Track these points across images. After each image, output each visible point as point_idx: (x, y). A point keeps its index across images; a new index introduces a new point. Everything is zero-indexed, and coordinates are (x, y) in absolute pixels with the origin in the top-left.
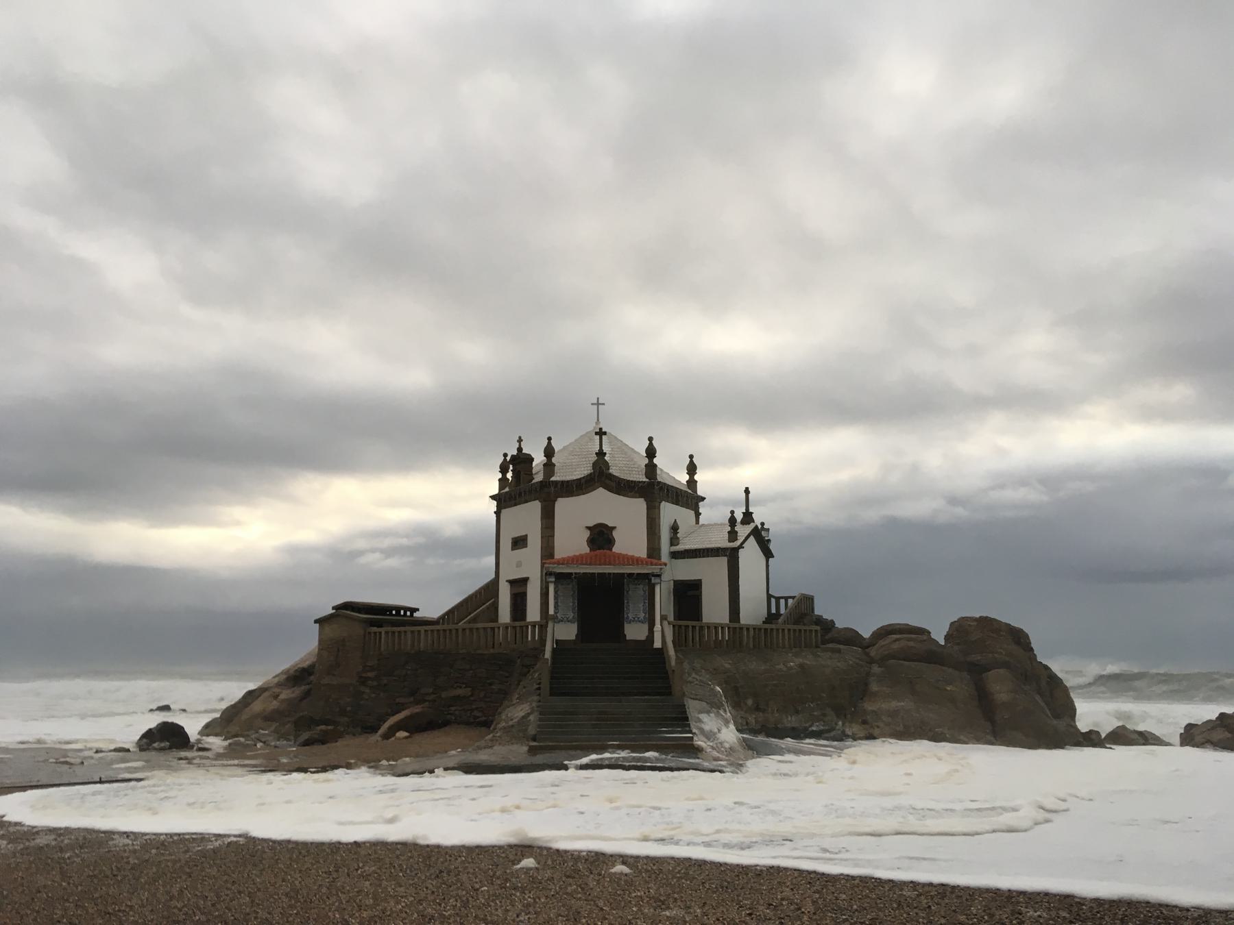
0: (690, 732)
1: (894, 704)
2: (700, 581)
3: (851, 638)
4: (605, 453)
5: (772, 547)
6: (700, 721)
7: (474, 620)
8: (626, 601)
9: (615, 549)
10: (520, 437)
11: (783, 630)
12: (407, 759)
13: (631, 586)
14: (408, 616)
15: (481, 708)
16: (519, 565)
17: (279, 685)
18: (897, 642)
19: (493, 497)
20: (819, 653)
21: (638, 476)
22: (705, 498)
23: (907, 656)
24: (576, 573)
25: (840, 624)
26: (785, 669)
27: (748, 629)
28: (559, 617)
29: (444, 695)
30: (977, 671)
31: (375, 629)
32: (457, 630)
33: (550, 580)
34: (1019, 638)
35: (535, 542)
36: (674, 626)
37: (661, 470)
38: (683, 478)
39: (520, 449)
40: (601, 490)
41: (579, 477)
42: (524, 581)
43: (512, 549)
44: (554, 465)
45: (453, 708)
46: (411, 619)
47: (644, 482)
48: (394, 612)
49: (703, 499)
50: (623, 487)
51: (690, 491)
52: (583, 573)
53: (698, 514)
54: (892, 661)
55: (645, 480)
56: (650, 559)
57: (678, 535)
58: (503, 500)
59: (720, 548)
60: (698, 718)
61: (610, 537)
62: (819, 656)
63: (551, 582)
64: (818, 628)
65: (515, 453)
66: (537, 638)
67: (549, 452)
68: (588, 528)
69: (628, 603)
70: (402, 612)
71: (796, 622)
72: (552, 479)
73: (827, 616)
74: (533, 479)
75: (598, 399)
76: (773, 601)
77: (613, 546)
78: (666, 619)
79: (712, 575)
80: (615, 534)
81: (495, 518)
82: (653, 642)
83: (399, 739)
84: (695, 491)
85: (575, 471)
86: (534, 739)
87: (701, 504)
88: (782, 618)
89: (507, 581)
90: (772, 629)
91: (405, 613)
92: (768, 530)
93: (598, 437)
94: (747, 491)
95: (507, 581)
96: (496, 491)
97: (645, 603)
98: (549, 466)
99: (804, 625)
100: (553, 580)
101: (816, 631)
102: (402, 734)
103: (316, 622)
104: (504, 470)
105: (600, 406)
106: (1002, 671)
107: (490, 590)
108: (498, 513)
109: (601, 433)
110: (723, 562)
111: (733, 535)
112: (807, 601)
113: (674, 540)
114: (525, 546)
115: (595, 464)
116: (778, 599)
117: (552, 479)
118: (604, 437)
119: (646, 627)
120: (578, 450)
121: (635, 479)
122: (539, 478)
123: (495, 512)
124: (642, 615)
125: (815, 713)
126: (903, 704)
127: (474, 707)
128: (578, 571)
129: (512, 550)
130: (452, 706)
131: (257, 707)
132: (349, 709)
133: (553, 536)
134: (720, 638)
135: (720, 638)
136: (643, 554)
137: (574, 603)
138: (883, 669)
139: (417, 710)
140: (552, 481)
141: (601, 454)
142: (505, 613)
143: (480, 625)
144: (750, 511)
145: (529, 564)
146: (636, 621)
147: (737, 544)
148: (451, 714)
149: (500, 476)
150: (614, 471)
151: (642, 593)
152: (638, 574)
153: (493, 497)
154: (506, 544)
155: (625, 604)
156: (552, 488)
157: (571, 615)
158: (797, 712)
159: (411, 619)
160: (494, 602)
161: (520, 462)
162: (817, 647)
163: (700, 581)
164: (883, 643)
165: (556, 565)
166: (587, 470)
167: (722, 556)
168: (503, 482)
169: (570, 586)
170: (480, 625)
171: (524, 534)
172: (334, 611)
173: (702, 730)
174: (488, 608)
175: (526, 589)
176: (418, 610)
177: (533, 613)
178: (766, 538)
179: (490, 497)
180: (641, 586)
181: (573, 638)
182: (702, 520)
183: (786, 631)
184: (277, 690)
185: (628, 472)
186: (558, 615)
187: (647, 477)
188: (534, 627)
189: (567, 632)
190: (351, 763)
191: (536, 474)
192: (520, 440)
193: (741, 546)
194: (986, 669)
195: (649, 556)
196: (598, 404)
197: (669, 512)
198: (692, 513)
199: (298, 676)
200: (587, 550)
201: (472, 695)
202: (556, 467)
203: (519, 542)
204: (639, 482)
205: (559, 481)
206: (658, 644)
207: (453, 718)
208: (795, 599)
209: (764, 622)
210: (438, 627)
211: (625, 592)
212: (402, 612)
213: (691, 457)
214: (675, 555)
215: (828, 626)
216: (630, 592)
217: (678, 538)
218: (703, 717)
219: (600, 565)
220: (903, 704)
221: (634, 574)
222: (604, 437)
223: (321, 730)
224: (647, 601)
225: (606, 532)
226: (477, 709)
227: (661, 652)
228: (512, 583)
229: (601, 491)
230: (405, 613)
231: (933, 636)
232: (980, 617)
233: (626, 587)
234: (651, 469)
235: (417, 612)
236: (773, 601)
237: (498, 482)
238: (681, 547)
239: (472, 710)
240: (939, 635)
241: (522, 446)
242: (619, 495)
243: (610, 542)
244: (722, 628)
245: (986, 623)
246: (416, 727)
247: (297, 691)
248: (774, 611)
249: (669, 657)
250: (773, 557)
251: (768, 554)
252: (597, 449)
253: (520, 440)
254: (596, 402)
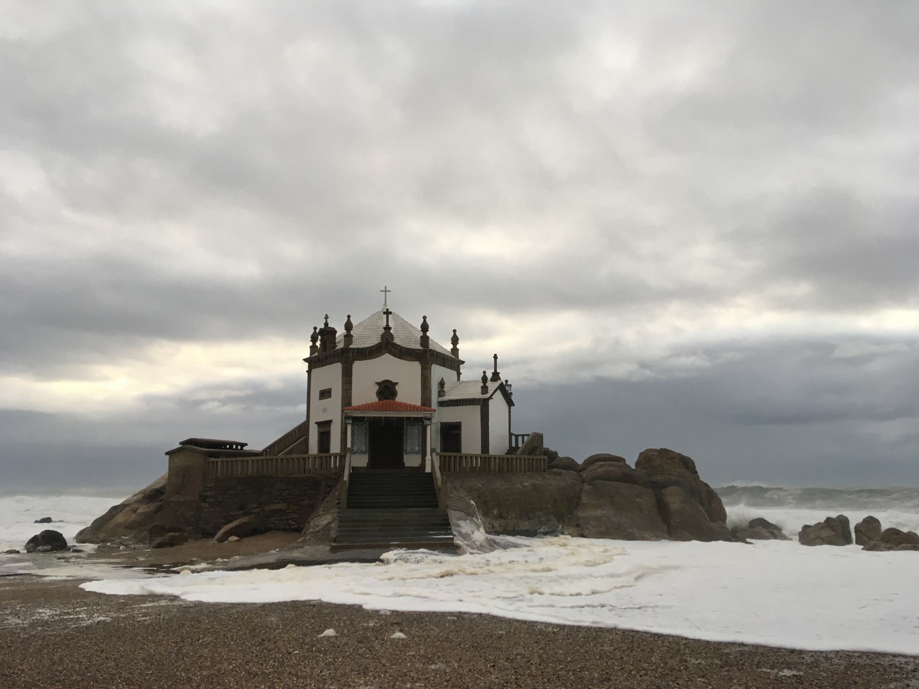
0: (451, 534)
1: (599, 512)
2: (460, 423)
3: (569, 465)
4: (391, 328)
5: (513, 398)
6: (459, 526)
7: (290, 452)
8: (405, 438)
10: (326, 315)
11: (520, 459)
12: (237, 557)
13: (409, 426)
14: (239, 450)
15: (295, 518)
16: (325, 410)
17: (136, 502)
18: (602, 467)
19: (305, 360)
20: (546, 476)
21: (415, 345)
22: (464, 362)
23: (609, 478)
24: (367, 417)
25: (561, 455)
26: (521, 488)
27: (495, 458)
28: (355, 450)
29: (266, 508)
30: (658, 488)
31: (213, 459)
32: (277, 460)
33: (349, 422)
34: (687, 464)
35: (337, 394)
36: (440, 456)
37: (432, 340)
38: (449, 347)
39: (326, 324)
40: (387, 355)
41: (371, 346)
42: (328, 423)
43: (320, 399)
44: (352, 336)
45: (274, 519)
46: (242, 451)
47: (420, 350)
48: (228, 447)
49: (463, 362)
50: (403, 353)
51: (453, 357)
52: (373, 417)
53: (459, 374)
54: (598, 481)
55: (420, 348)
56: (423, 407)
57: (445, 389)
58: (313, 362)
59: (475, 399)
60: (458, 524)
61: (394, 390)
62: (546, 478)
63: (349, 423)
64: (546, 457)
65: (323, 326)
66: (337, 466)
67: (349, 326)
68: (377, 383)
69: (406, 439)
70: (234, 447)
71: (529, 454)
72: (351, 346)
73: (552, 448)
74: (337, 346)
75: (386, 287)
76: (513, 437)
77: (396, 397)
78: (435, 451)
79: (469, 419)
80: (397, 388)
81: (307, 376)
82: (425, 469)
83: (231, 542)
84: (457, 355)
85: (368, 341)
86: (335, 541)
87: (461, 366)
88: (520, 449)
89: (316, 423)
90: (512, 459)
91: (237, 447)
92: (510, 386)
93: (385, 316)
94: (495, 357)
95: (316, 423)
96: (307, 355)
97: (419, 439)
98: (348, 337)
99: (536, 455)
100: (351, 422)
101: (544, 459)
102: (233, 538)
103: (167, 454)
104: (314, 339)
105: (387, 293)
106: (675, 488)
107: (303, 429)
108: (309, 372)
109: (388, 313)
110: (477, 409)
111: (485, 389)
112: (538, 438)
113: (441, 393)
114: (330, 397)
115: (383, 336)
116: (517, 436)
117: (351, 346)
118: (390, 316)
119: (420, 456)
120: (370, 325)
121: (412, 347)
122: (340, 346)
123: (307, 371)
124: (417, 448)
125: (542, 519)
126: (605, 512)
127: (289, 517)
128: (369, 415)
129: (320, 399)
130: (272, 517)
131: (120, 518)
132: (192, 520)
133: (351, 389)
134: (474, 465)
135: (474, 465)
136: (418, 402)
137: (366, 439)
138: (590, 487)
139: (246, 521)
140: (350, 348)
141: (387, 328)
142: (313, 447)
143: (293, 456)
144: (498, 371)
145: (332, 410)
146: (413, 453)
147: (488, 395)
148: (271, 523)
149: (311, 344)
150: (397, 341)
151: (418, 431)
152: (414, 418)
153: (305, 360)
154: (315, 395)
155: (404, 440)
156: (351, 354)
157: (364, 448)
158: (530, 519)
159: (242, 451)
160: (305, 439)
161: (327, 333)
162: (544, 471)
163: (460, 423)
164: (592, 468)
165: (353, 411)
166: (378, 340)
167: (477, 404)
168: (313, 348)
169: (364, 427)
170: (293, 456)
171: (329, 388)
172: (181, 446)
173: (460, 533)
174: (301, 443)
175: (330, 429)
176: (247, 444)
177: (335, 447)
178: (509, 392)
179: (304, 360)
180: (417, 426)
181: (365, 465)
182: (461, 379)
183: (523, 460)
184: (136, 506)
185: (407, 342)
186: (354, 448)
187: (421, 346)
188: (335, 457)
189: (361, 461)
190: (193, 561)
191: (339, 342)
192: (326, 317)
193: (491, 398)
194: (665, 486)
195: (423, 404)
196: (386, 291)
197: (438, 372)
198: (455, 372)
199: (152, 495)
200: (376, 400)
201: (288, 509)
202: (353, 338)
203: (325, 394)
204: (416, 350)
205: (356, 348)
206: (428, 469)
207: (273, 526)
208: (529, 436)
209: (506, 453)
210: (260, 458)
211: (405, 432)
212: (234, 447)
213: (455, 331)
214: (442, 404)
215: (552, 456)
216: (408, 431)
217: (444, 391)
218: (462, 523)
219: (386, 411)
220: (605, 512)
221: (411, 417)
222: (390, 316)
223: (170, 536)
224: (421, 438)
225: (390, 386)
226: (291, 519)
227: (431, 475)
228: (319, 424)
229: (387, 357)
230: (237, 447)
231: (627, 463)
232: (661, 449)
233: (405, 427)
234: (425, 340)
235: (246, 446)
236: (513, 437)
237: (309, 349)
238: (446, 398)
239: (288, 520)
240: (631, 462)
241: (328, 322)
242: (400, 359)
243: (394, 394)
244: (476, 458)
245: (664, 453)
246: (244, 533)
247: (153, 506)
248: (514, 445)
249: (436, 479)
250: (514, 405)
251: (510, 403)
252: (385, 325)
253: (326, 317)
254: (384, 289)
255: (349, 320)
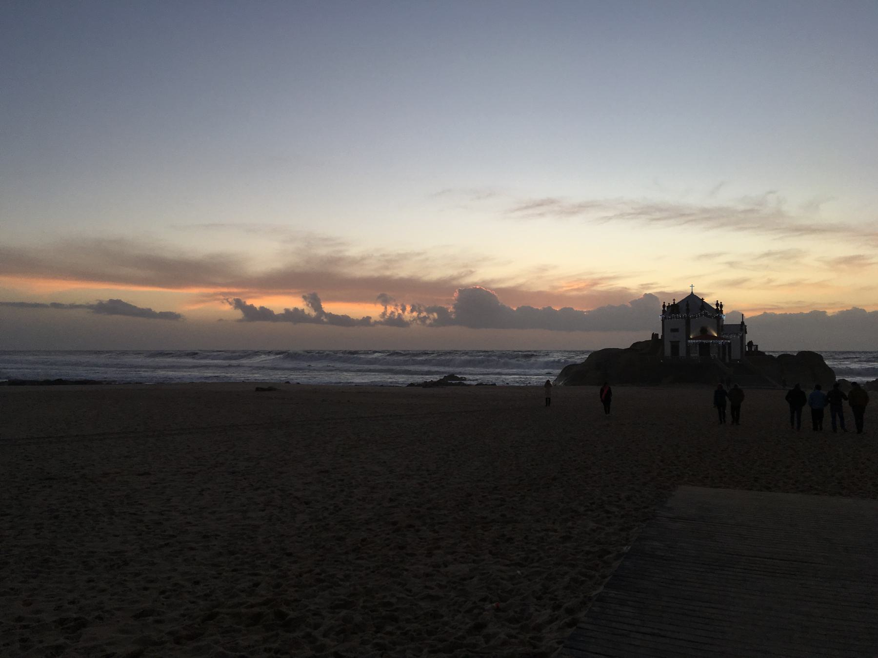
9: (708, 333)
39: (674, 303)
42: (679, 341)
65: (673, 304)
67: (688, 305)
98: (688, 310)
104: (664, 306)
108: (663, 320)
149: (663, 309)
168: (664, 311)
177: (682, 352)
192: (674, 300)
196: (692, 286)
203: (675, 330)
228: (671, 342)
234: (717, 308)
255: (687, 301)
